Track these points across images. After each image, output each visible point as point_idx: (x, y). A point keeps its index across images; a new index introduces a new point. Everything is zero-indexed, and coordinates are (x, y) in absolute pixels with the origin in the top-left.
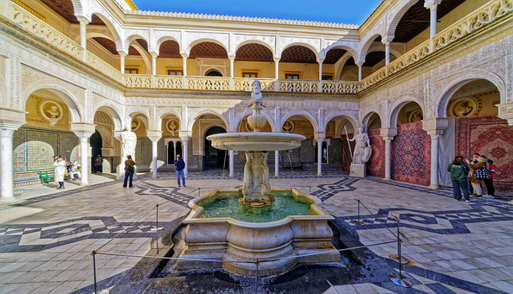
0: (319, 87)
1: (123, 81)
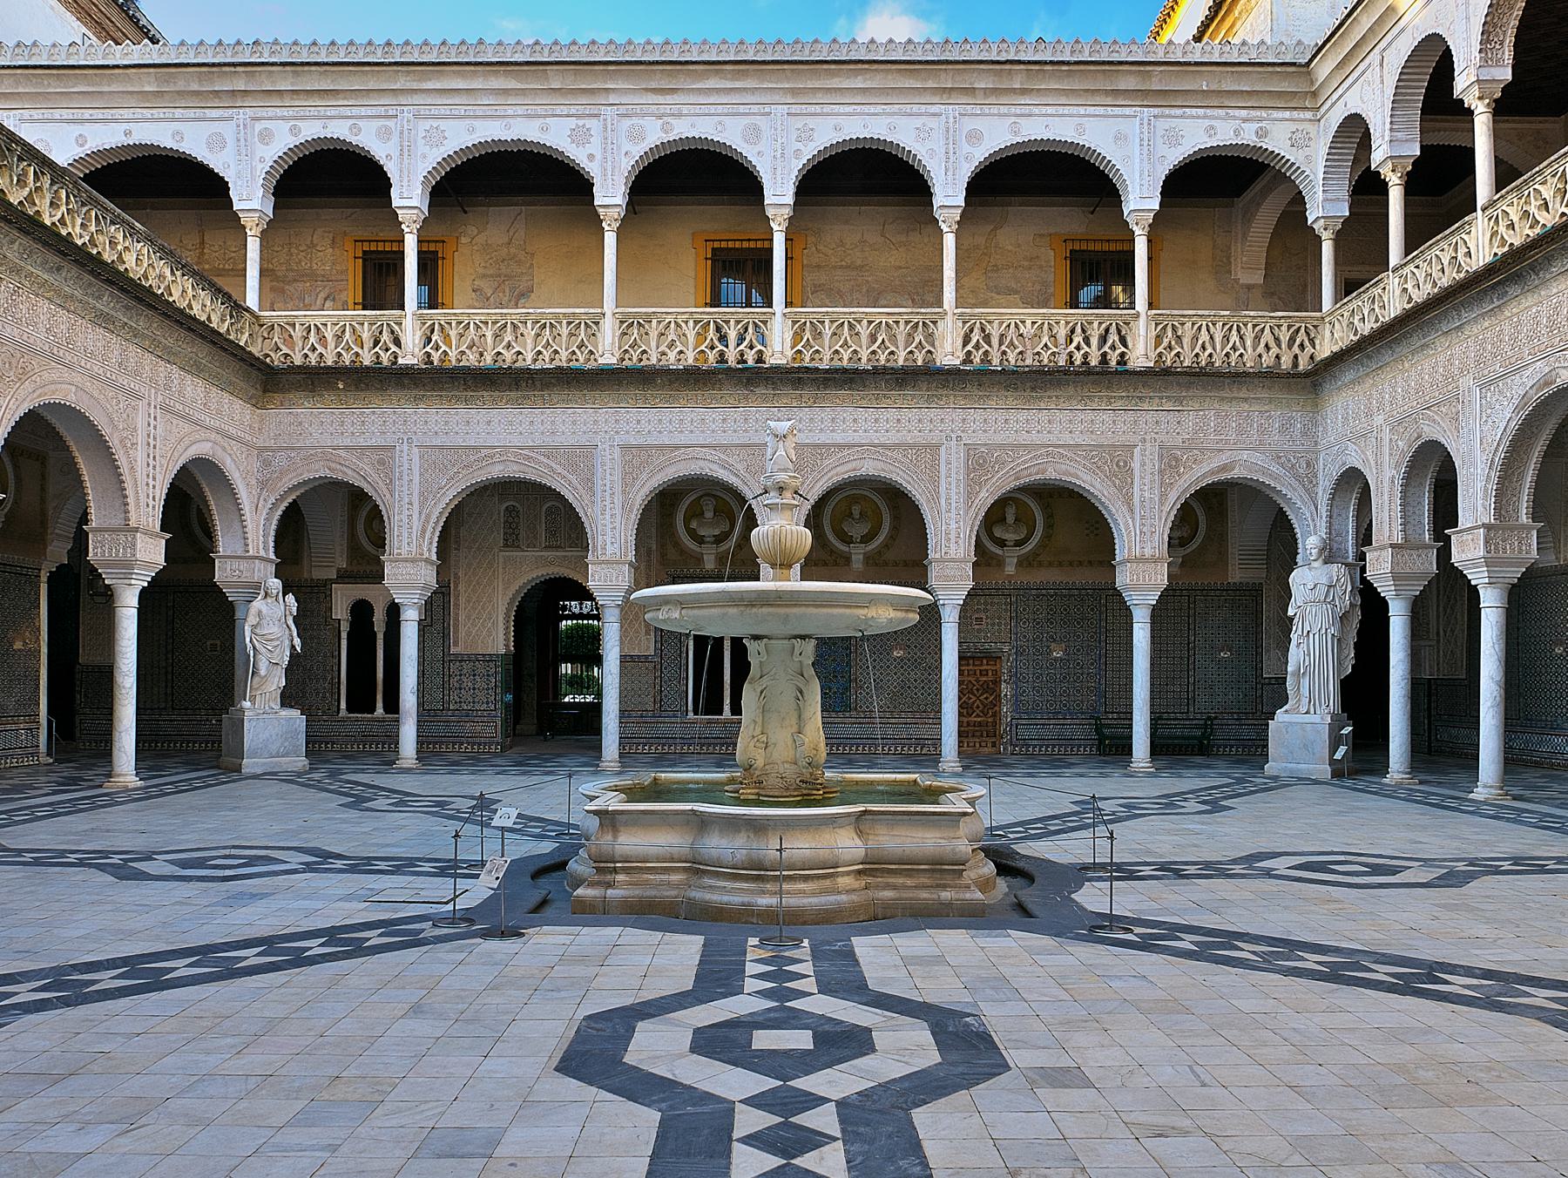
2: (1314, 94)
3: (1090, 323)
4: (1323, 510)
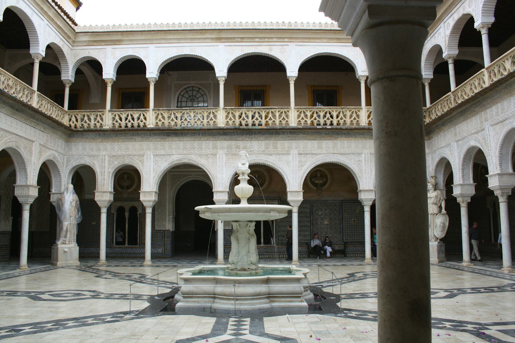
0: (361, 118)
1: (65, 121)
2: (74, 42)
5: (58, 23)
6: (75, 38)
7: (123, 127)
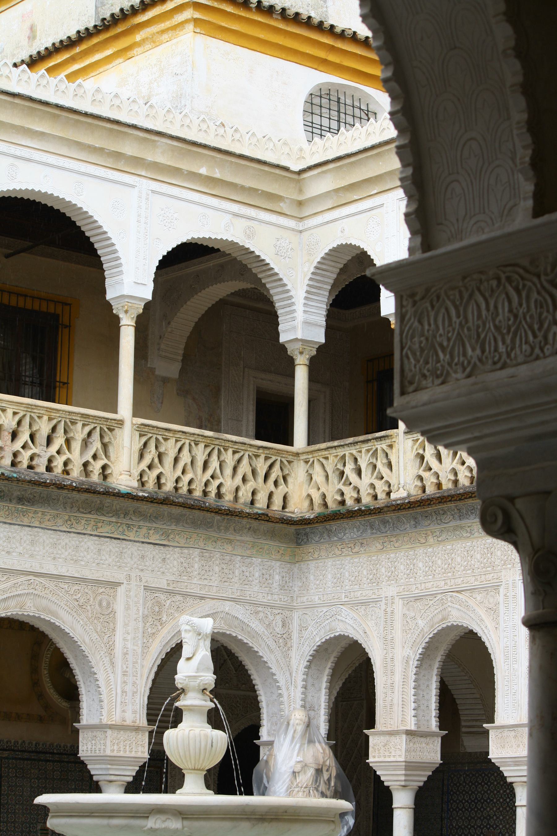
3: (74, 423)
4: (299, 678)
5: (203, 171)
6: (301, 191)
7: (447, 485)
